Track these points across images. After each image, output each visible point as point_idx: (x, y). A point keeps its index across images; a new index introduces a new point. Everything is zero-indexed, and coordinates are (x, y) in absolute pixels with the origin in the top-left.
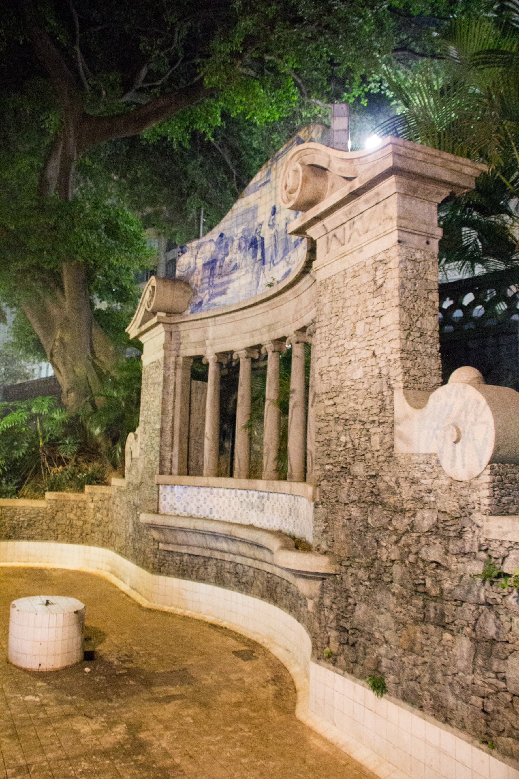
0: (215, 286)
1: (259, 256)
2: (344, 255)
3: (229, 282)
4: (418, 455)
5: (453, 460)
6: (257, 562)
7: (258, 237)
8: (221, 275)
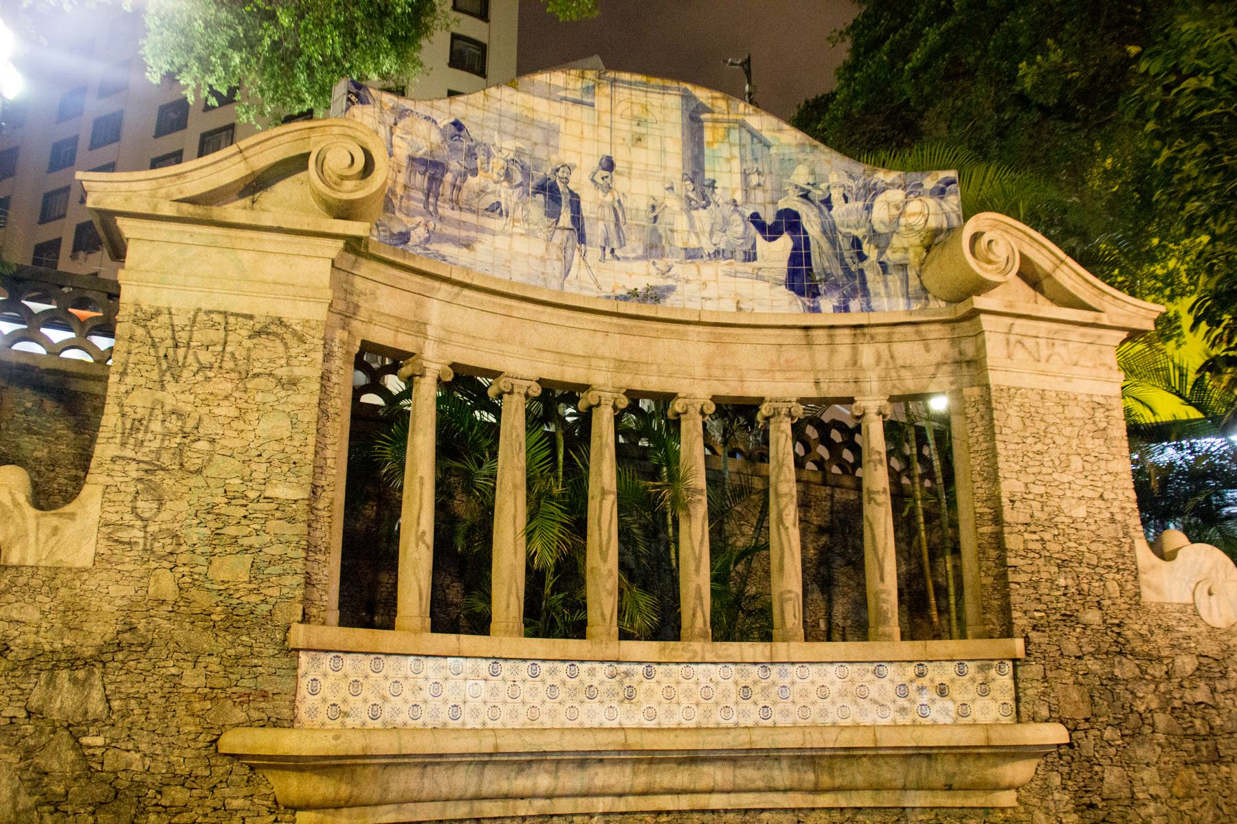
0: (441, 219)
1: (565, 218)
2: (1044, 373)
3: (481, 229)
4: (1172, 604)
5: (1210, 609)
6: (630, 798)
7: (560, 186)
8: (455, 203)
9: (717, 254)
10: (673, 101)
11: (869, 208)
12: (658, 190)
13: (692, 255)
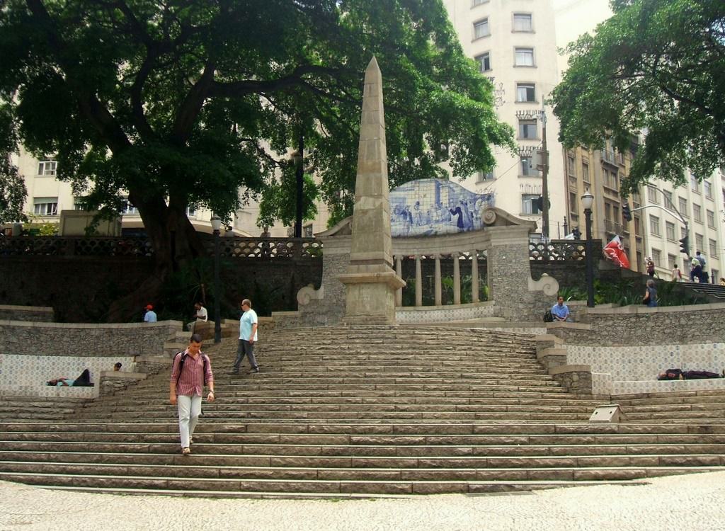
1: (408, 219)
9: (443, 220)
10: (433, 184)
11: (475, 204)
12: (429, 207)
13: (437, 222)
